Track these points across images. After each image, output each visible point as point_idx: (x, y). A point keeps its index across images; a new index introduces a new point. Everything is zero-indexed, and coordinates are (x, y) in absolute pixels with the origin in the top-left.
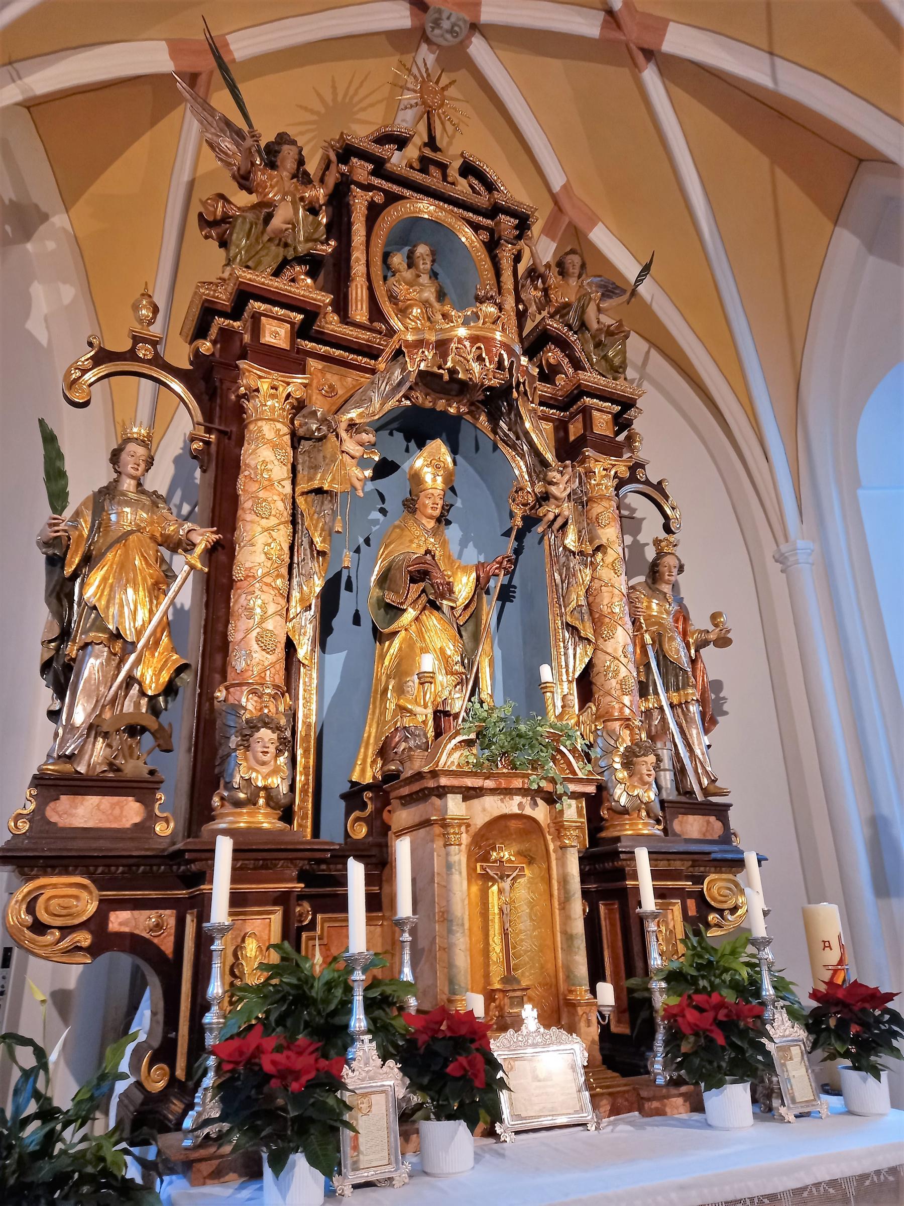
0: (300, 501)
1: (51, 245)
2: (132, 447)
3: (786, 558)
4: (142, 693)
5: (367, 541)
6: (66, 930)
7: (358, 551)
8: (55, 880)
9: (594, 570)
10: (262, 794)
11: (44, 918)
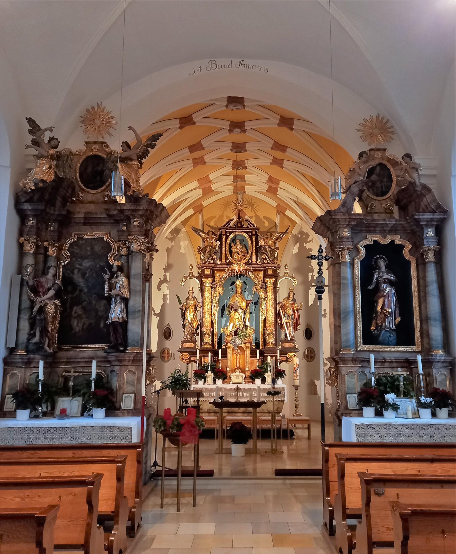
0: (213, 298)
1: (182, 235)
2: (190, 291)
5: (230, 298)
6: (186, 359)
7: (228, 300)
11: (183, 358)
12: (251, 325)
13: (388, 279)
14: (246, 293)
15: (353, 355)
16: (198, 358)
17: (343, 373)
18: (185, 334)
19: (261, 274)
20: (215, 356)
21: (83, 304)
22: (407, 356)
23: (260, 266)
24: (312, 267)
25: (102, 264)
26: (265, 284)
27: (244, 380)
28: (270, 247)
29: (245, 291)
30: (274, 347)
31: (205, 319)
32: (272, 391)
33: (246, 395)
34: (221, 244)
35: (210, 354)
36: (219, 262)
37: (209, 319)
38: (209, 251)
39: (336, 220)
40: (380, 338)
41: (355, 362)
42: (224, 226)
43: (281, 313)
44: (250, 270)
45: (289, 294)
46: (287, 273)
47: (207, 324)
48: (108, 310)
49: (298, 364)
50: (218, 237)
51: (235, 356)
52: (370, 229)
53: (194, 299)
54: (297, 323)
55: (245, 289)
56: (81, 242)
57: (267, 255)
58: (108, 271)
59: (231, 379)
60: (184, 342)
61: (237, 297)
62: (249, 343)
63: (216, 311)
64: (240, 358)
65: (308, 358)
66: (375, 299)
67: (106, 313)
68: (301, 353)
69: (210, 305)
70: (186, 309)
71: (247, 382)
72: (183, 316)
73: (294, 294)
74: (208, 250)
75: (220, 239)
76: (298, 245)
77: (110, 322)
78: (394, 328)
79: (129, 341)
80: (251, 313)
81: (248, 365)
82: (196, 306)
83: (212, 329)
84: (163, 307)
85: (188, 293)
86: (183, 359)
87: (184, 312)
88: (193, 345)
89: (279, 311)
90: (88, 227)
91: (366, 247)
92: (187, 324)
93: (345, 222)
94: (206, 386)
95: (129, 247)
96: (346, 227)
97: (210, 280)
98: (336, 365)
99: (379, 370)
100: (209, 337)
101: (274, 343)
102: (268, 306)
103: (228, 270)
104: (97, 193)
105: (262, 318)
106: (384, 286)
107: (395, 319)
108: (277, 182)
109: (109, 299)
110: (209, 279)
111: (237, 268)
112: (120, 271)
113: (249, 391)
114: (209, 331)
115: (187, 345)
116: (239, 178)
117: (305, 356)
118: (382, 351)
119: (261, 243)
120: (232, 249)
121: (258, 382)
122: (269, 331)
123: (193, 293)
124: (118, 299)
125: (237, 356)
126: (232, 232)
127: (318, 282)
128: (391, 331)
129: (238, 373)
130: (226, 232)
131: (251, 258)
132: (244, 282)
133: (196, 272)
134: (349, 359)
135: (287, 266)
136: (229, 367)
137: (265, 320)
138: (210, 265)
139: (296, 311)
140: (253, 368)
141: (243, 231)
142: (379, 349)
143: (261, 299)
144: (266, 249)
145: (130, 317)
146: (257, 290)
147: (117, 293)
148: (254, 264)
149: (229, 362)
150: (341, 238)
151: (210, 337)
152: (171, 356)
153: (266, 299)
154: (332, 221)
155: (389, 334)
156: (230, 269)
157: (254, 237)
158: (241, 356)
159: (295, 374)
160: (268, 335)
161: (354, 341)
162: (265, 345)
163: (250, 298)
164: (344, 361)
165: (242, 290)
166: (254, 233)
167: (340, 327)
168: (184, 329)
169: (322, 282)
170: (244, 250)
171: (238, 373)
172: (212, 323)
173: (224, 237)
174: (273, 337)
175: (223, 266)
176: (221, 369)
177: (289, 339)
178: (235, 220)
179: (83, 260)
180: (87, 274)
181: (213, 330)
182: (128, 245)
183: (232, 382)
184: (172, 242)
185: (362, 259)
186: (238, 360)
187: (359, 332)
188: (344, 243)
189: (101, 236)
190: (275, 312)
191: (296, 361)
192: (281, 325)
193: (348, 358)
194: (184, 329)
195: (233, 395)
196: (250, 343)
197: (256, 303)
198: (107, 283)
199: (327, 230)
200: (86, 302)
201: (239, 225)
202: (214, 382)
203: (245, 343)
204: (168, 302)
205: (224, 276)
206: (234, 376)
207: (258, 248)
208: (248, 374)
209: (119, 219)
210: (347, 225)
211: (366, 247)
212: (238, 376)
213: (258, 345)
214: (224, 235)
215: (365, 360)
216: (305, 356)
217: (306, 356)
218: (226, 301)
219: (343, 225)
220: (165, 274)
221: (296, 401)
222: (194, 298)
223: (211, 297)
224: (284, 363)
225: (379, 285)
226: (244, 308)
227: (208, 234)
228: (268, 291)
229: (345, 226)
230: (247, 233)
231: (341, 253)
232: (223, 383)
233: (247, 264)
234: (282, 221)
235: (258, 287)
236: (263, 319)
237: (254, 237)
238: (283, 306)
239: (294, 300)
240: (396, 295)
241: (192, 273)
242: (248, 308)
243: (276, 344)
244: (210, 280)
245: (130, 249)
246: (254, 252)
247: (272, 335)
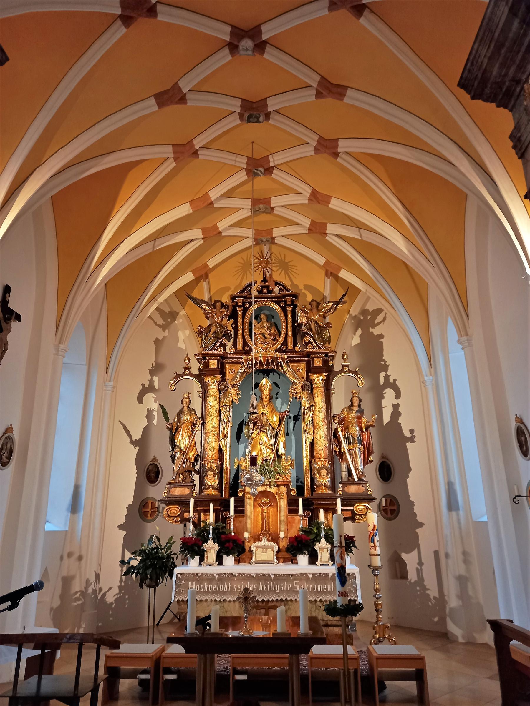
0: (221, 408)
1: (181, 321)
3: (426, 382)
4: (190, 462)
6: (175, 517)
8: (172, 506)
9: (313, 412)
10: (211, 487)
12: (287, 453)
14: (279, 401)
16: (191, 514)
18: (174, 472)
19: (304, 365)
20: (226, 511)
23: (300, 354)
24: (385, 362)
26: (311, 383)
27: (277, 555)
28: (316, 322)
29: (277, 398)
30: (330, 492)
31: (207, 445)
32: (341, 602)
33: (280, 588)
34: (236, 323)
35: (212, 505)
36: (233, 350)
37: (215, 445)
38: (215, 332)
42: (242, 292)
43: (340, 433)
44: (283, 359)
45: (351, 401)
46: (347, 366)
47: (210, 452)
49: (376, 524)
51: (259, 509)
53: (191, 413)
54: (368, 451)
55: (277, 394)
57: (312, 337)
59: (252, 555)
61: (263, 408)
62: (284, 485)
63: (228, 431)
64: (268, 513)
65: (387, 513)
68: (375, 504)
69: (216, 421)
70: (177, 429)
71: (282, 560)
72: (172, 441)
73: (360, 401)
74: (213, 329)
75: (233, 316)
76: (359, 332)
80: (287, 434)
81: (283, 527)
82: (194, 424)
83: (219, 463)
84: (146, 431)
85: (182, 402)
86: (169, 516)
87: (175, 434)
88: (187, 491)
89: (336, 430)
92: (179, 454)
94: (204, 570)
97: (218, 378)
100: (214, 477)
101: (329, 484)
102: (317, 421)
103: (246, 360)
105: (306, 441)
108: (326, 200)
110: (215, 377)
111: (261, 355)
113: (285, 580)
114: (214, 466)
116: (262, 203)
117: (381, 509)
119: (301, 318)
121: (303, 559)
122: (320, 464)
123: (190, 402)
125: (263, 510)
129: (264, 542)
130: (244, 303)
131: (285, 343)
132: (275, 384)
133: (195, 367)
135: (346, 355)
136: (249, 530)
137: (312, 445)
139: (364, 430)
140: (293, 533)
141: (271, 301)
143: (304, 409)
144: (310, 326)
146: (297, 393)
148: (291, 351)
149: (249, 521)
151: (217, 476)
152: (159, 512)
153: (312, 406)
156: (250, 357)
157: (289, 309)
158: (271, 510)
159: (372, 544)
160: (319, 469)
162: (313, 490)
163: (285, 408)
165: (271, 395)
166: (289, 302)
168: (173, 462)
170: (274, 330)
171: (264, 542)
172: (220, 451)
173: (240, 310)
174: (327, 474)
175: (239, 355)
176: (233, 534)
177: (356, 479)
178: (259, 282)
181: (222, 464)
183: (254, 559)
184: (164, 331)
186: (266, 517)
190: (329, 429)
191: (373, 518)
192: (341, 455)
194: (173, 463)
195: (254, 588)
196: (287, 486)
197: (296, 418)
201: (265, 290)
202: (220, 562)
203: (278, 486)
204: (155, 422)
205: (240, 371)
206: (257, 549)
207: (296, 327)
208: (284, 544)
212: (265, 548)
213: (300, 490)
214: (240, 307)
216: (381, 509)
217: (384, 510)
218: (245, 415)
220: (152, 379)
221: (377, 598)
222: (192, 411)
223: (217, 406)
224: (349, 522)
226: (276, 426)
227: (214, 306)
228: (316, 395)
230: (278, 303)
232: (237, 561)
233: (280, 350)
234: (333, 291)
235: (299, 389)
236: (308, 444)
237: (289, 309)
238: (342, 422)
239: (361, 411)
241: (189, 369)
242: (283, 426)
243: (333, 488)
244: (218, 378)
246: (290, 333)
247: (325, 470)
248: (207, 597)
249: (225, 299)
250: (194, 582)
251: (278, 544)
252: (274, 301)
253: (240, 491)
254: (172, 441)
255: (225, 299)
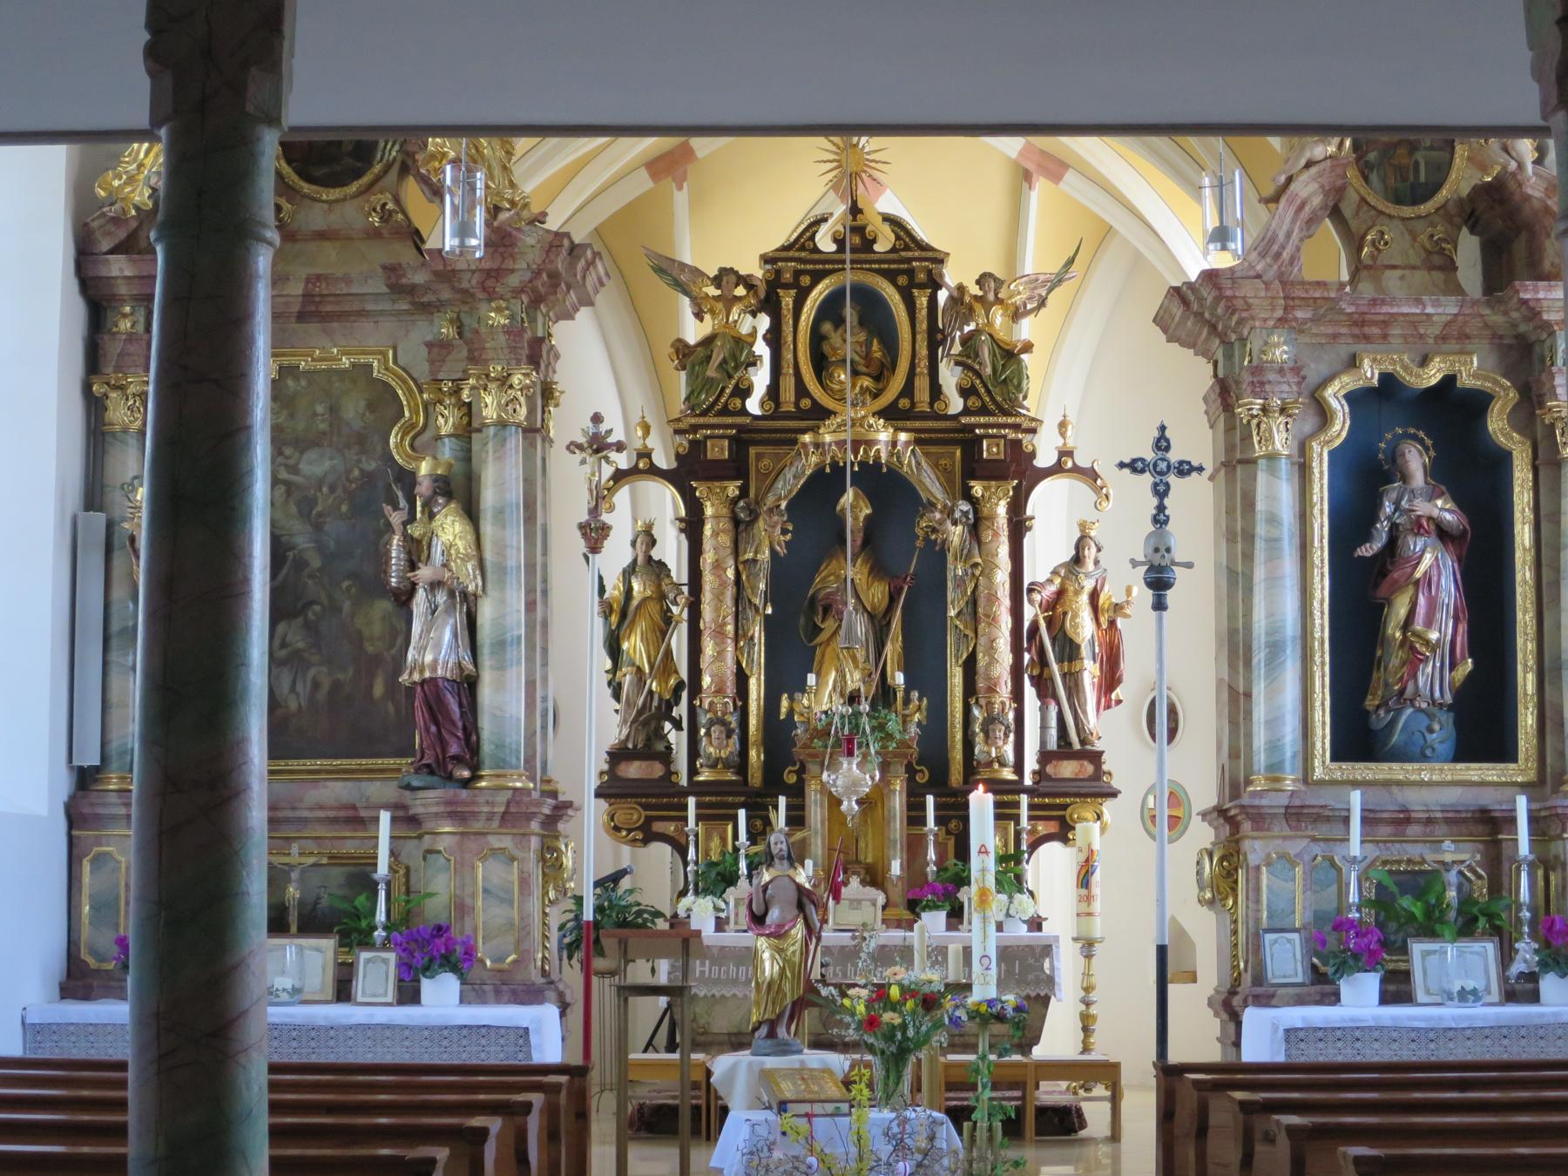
0: (741, 567)
13: (1430, 518)
15: (1291, 796)
17: (1253, 859)
21: (310, 615)
22: (1488, 799)
25: (371, 466)
39: (1239, 303)
40: (1396, 738)
41: (1299, 821)
46: (1070, 454)
48: (401, 634)
50: (762, 295)
52: (1366, 330)
56: (290, 383)
58: (400, 494)
60: (618, 755)
66: (1382, 591)
67: (392, 645)
75: (770, 304)
77: (416, 677)
78: (1448, 698)
79: (487, 748)
88: (657, 770)
90: (313, 327)
91: (1352, 398)
93: (1273, 309)
95: (469, 405)
96: (1275, 327)
97: (733, 489)
98: (1232, 834)
99: (1388, 849)
100: (729, 736)
104: (344, 199)
106: (1416, 544)
107: (1453, 666)
109: (404, 598)
112: (443, 495)
115: (633, 770)
118: (1399, 783)
120: (826, 349)
124: (441, 598)
126: (826, 274)
127: (1157, 550)
128: (1435, 710)
130: (797, 274)
134: (1276, 811)
138: (729, 420)
142: (1388, 777)
145: (486, 660)
147: (436, 578)
148: (923, 416)
150: (1257, 370)
154: (1222, 304)
155: (1426, 722)
161: (1299, 746)
164: (1259, 818)
167: (1248, 695)
169: (1168, 550)
173: (787, 300)
179: (302, 453)
180: (316, 504)
182: (465, 396)
185: (1337, 443)
187: (1318, 715)
188: (1268, 388)
189: (363, 359)
193: (1271, 807)
198: (396, 540)
199: (1209, 334)
200: (317, 608)
209: (433, 298)
210: (1280, 320)
211: (1352, 398)
214: (787, 286)
215: (1337, 814)
219: (1265, 320)
222: (658, 569)
225: (1400, 542)
229: (1271, 323)
230: (890, 276)
231: (1258, 425)
233: (891, 414)
237: (922, 301)
240: (1459, 577)
245: (474, 409)
248: (735, 991)
249: (753, 268)
250: (707, 962)
251: (885, 891)
252: (876, 271)
253: (790, 772)
254: (614, 648)
255: (753, 268)
